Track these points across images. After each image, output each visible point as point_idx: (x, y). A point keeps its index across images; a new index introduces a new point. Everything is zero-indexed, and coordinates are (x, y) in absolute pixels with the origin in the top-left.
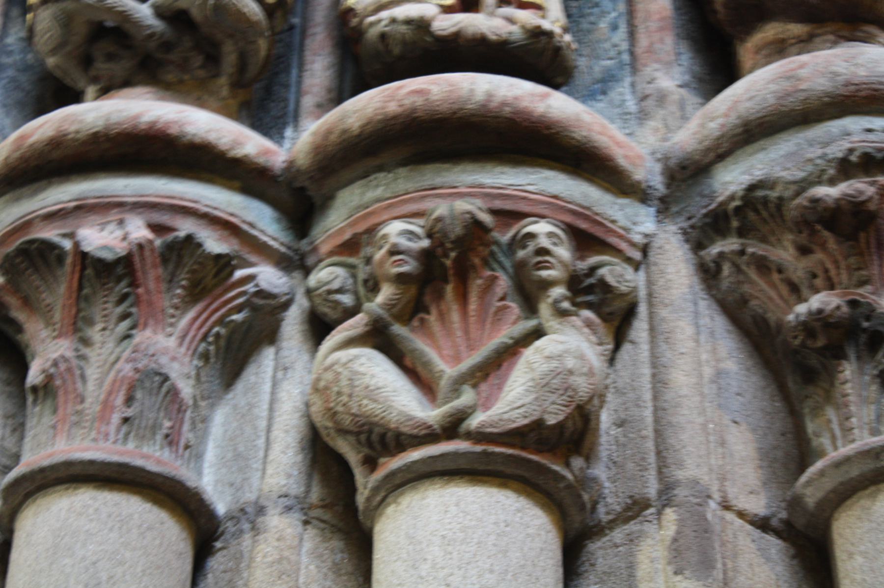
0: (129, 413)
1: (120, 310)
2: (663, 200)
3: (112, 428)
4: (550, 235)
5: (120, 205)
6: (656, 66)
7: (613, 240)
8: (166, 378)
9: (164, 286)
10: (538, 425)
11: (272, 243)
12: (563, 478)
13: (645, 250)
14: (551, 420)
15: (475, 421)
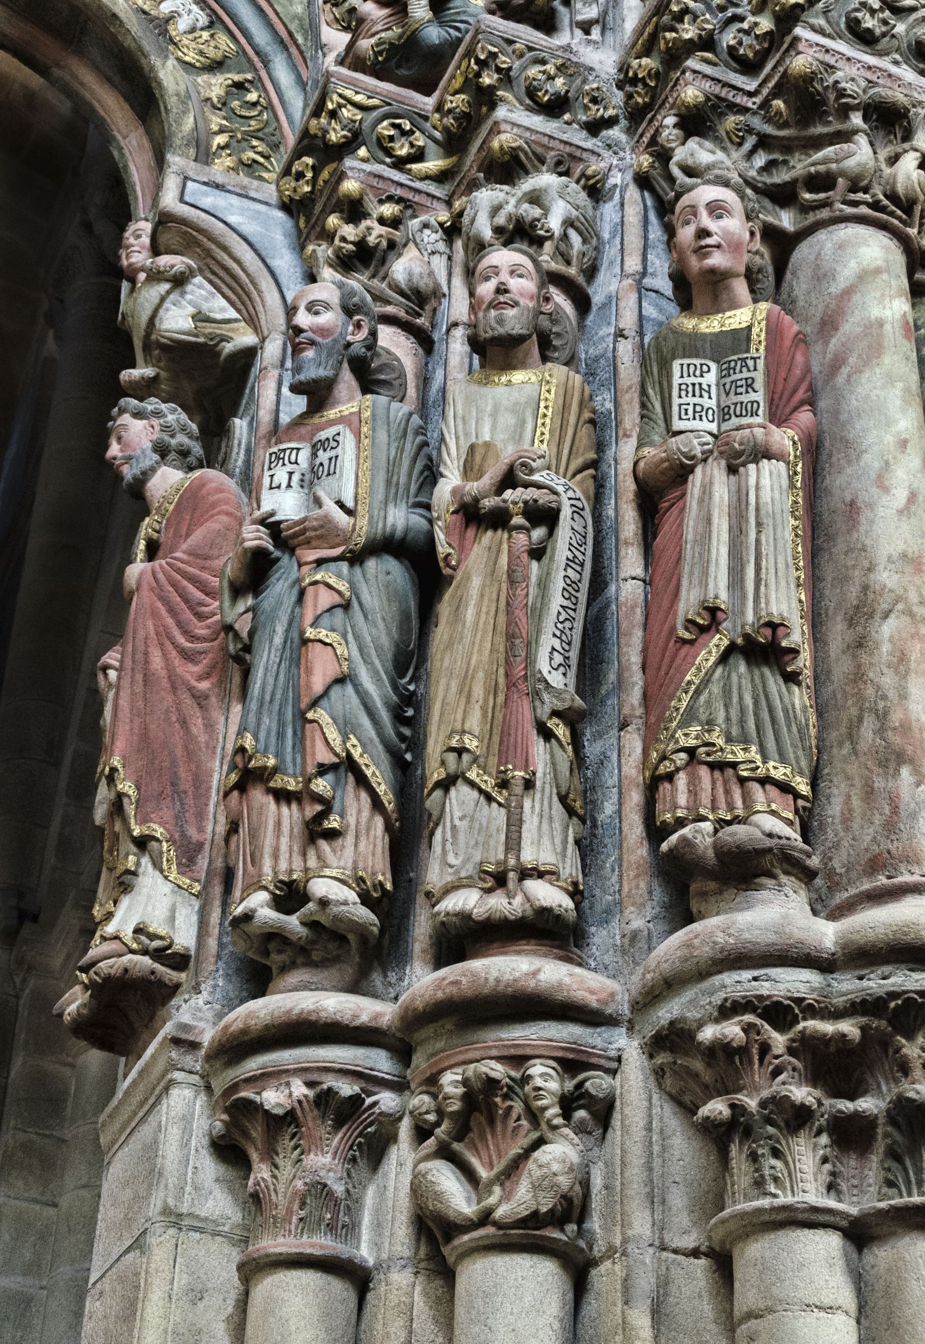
0: (302, 1213)
1: (292, 1143)
2: (630, 1021)
3: (293, 1227)
4: (542, 1075)
5: (287, 1071)
6: (632, 909)
7: (594, 1060)
8: (325, 1185)
9: (319, 1122)
10: (535, 1214)
11: (387, 1077)
12: (560, 1240)
13: (619, 1059)
14: (544, 1209)
15: (499, 1213)
